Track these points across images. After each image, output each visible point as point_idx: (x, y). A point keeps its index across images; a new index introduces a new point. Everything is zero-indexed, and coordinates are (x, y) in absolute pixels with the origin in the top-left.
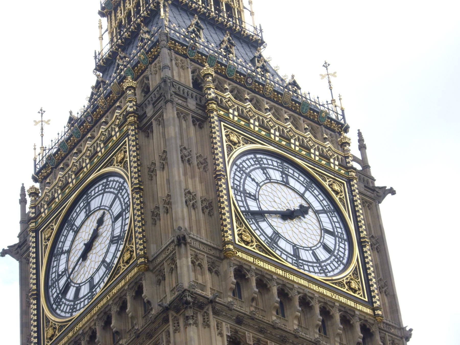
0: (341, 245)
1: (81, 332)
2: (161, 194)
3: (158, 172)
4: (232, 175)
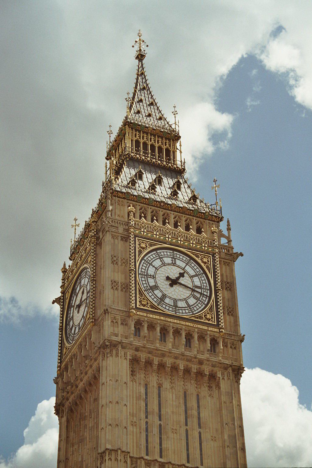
1: (73, 354)
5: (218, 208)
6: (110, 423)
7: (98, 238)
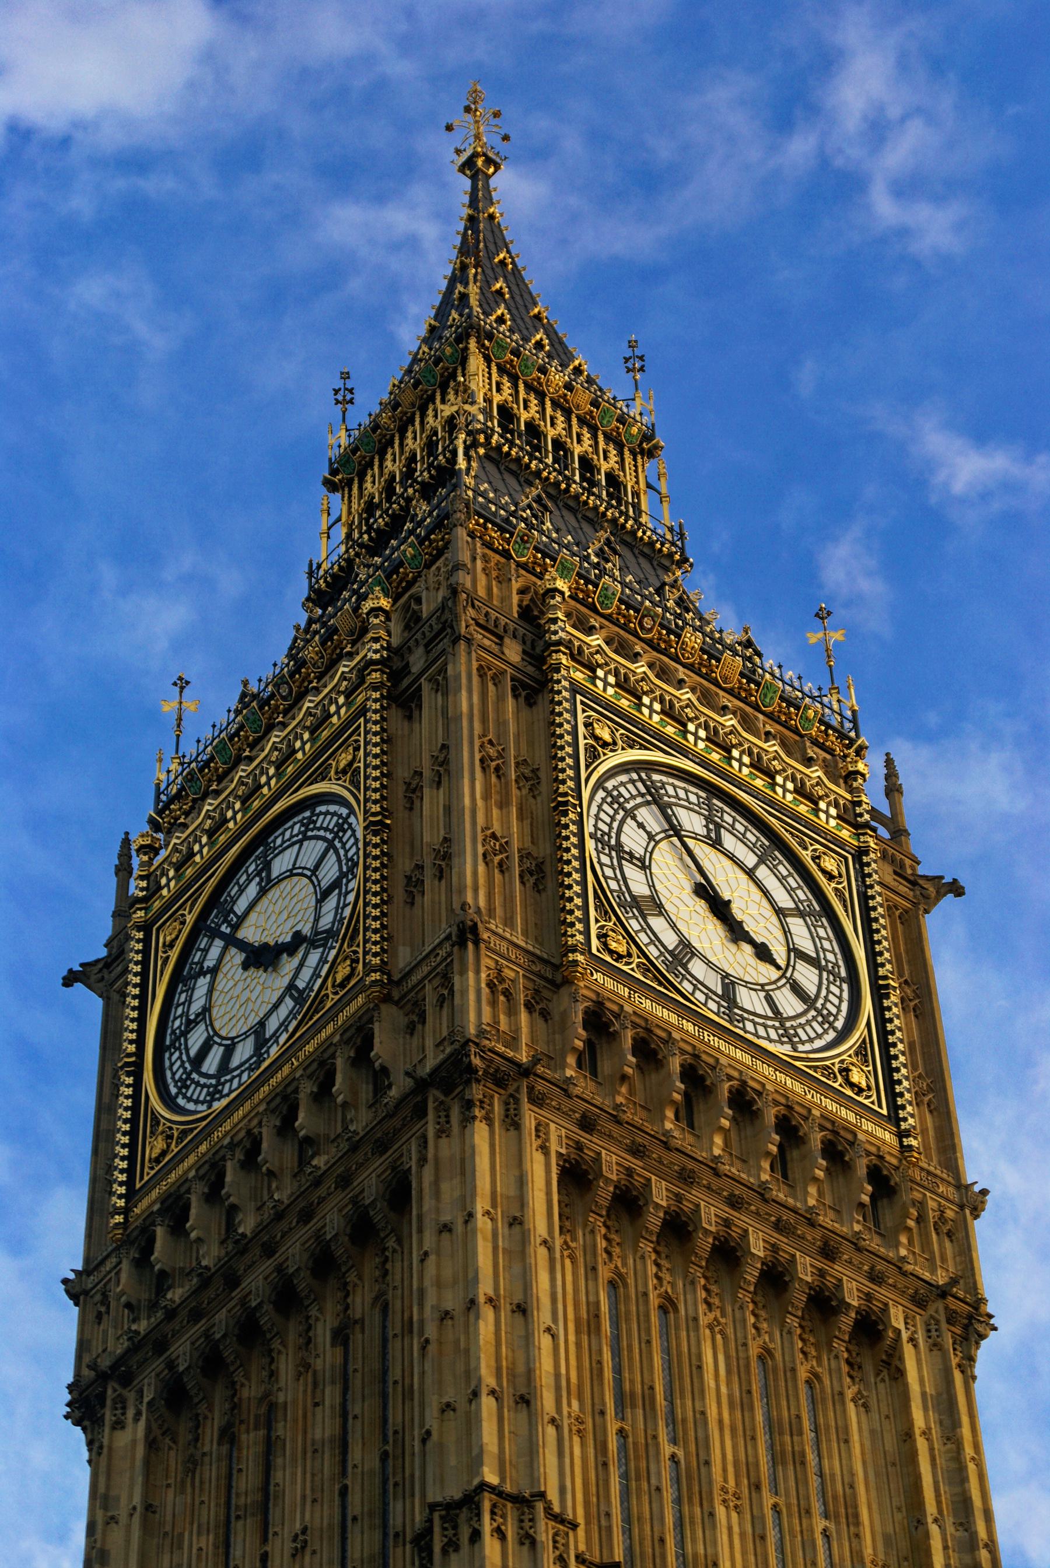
0: (833, 988)
2: (430, 836)
3: (426, 791)
4: (594, 810)
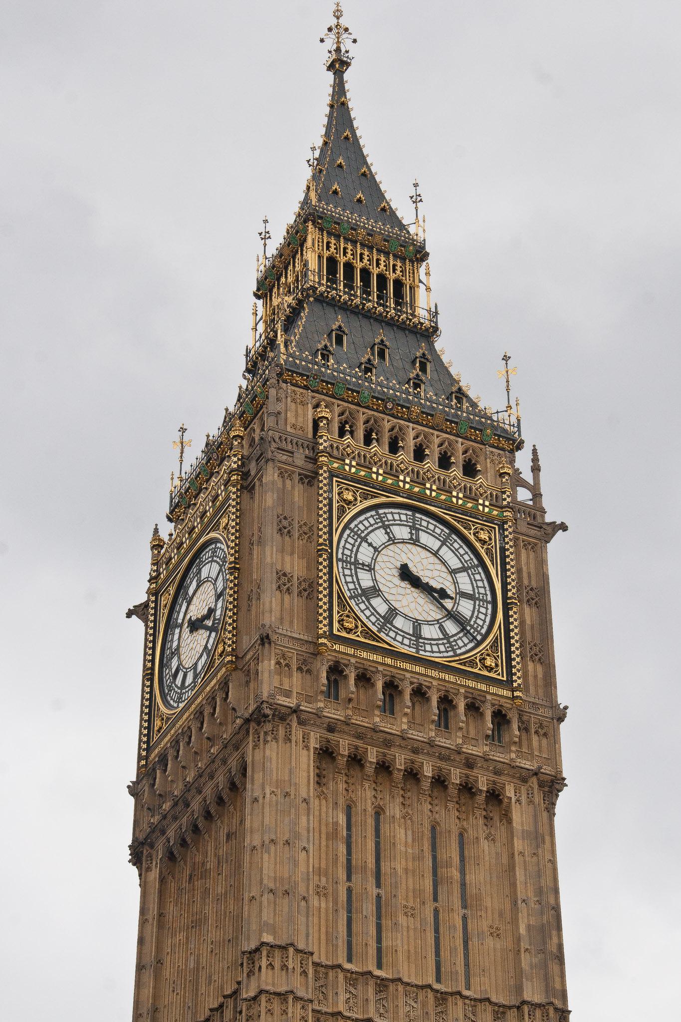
5: (514, 420)
6: (271, 885)
7: (245, 475)
